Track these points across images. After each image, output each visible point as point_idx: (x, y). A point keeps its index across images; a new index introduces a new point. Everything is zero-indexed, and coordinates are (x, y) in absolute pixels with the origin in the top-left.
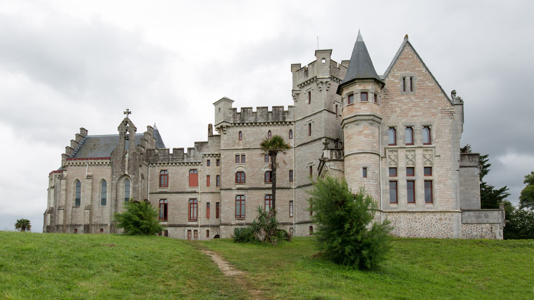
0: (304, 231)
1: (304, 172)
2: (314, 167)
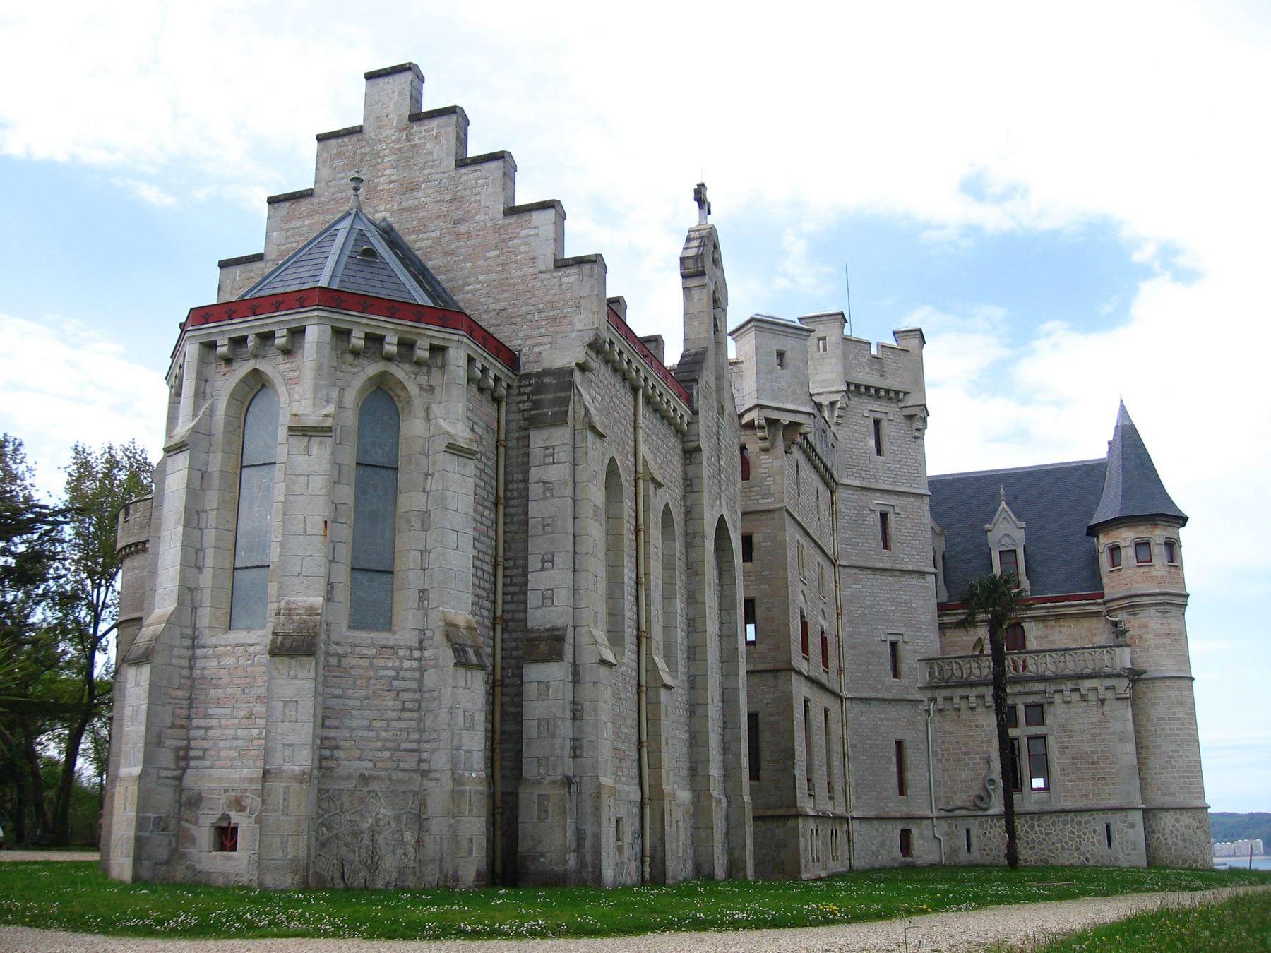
0: (883, 844)
1: (872, 652)
2: (907, 647)
